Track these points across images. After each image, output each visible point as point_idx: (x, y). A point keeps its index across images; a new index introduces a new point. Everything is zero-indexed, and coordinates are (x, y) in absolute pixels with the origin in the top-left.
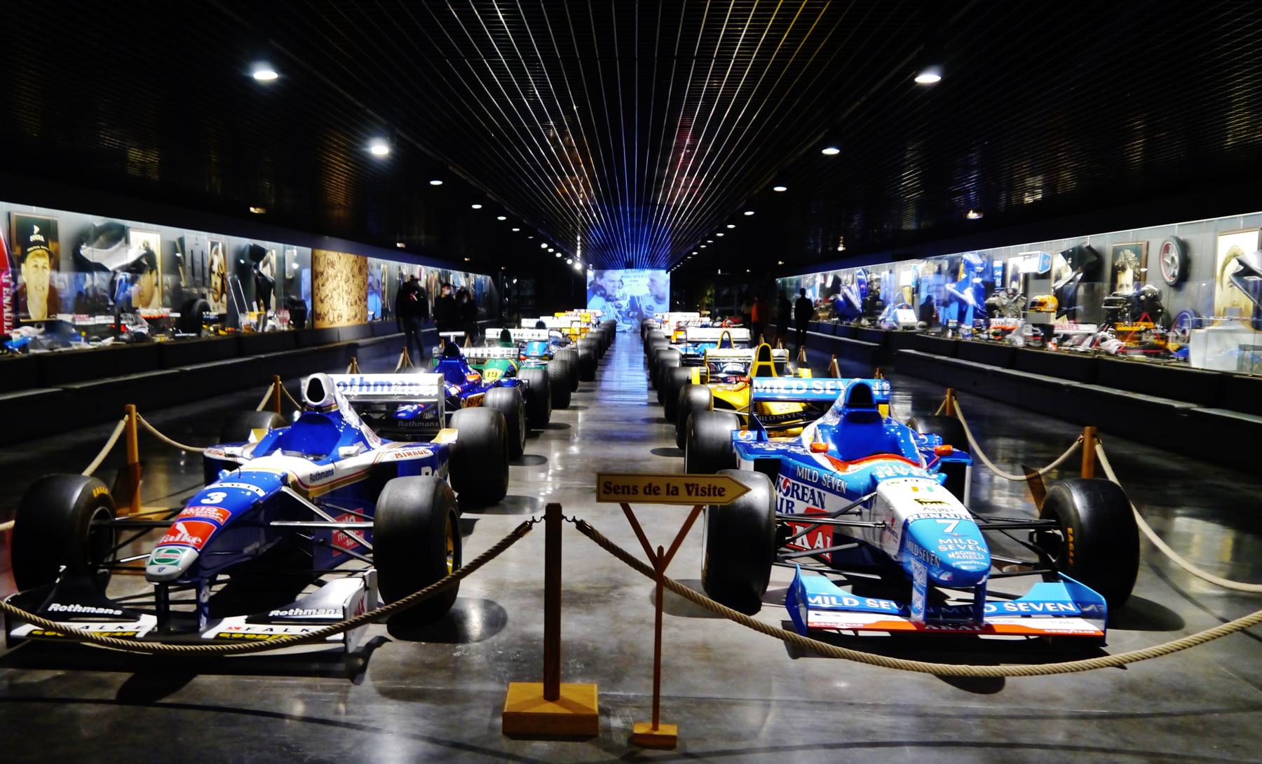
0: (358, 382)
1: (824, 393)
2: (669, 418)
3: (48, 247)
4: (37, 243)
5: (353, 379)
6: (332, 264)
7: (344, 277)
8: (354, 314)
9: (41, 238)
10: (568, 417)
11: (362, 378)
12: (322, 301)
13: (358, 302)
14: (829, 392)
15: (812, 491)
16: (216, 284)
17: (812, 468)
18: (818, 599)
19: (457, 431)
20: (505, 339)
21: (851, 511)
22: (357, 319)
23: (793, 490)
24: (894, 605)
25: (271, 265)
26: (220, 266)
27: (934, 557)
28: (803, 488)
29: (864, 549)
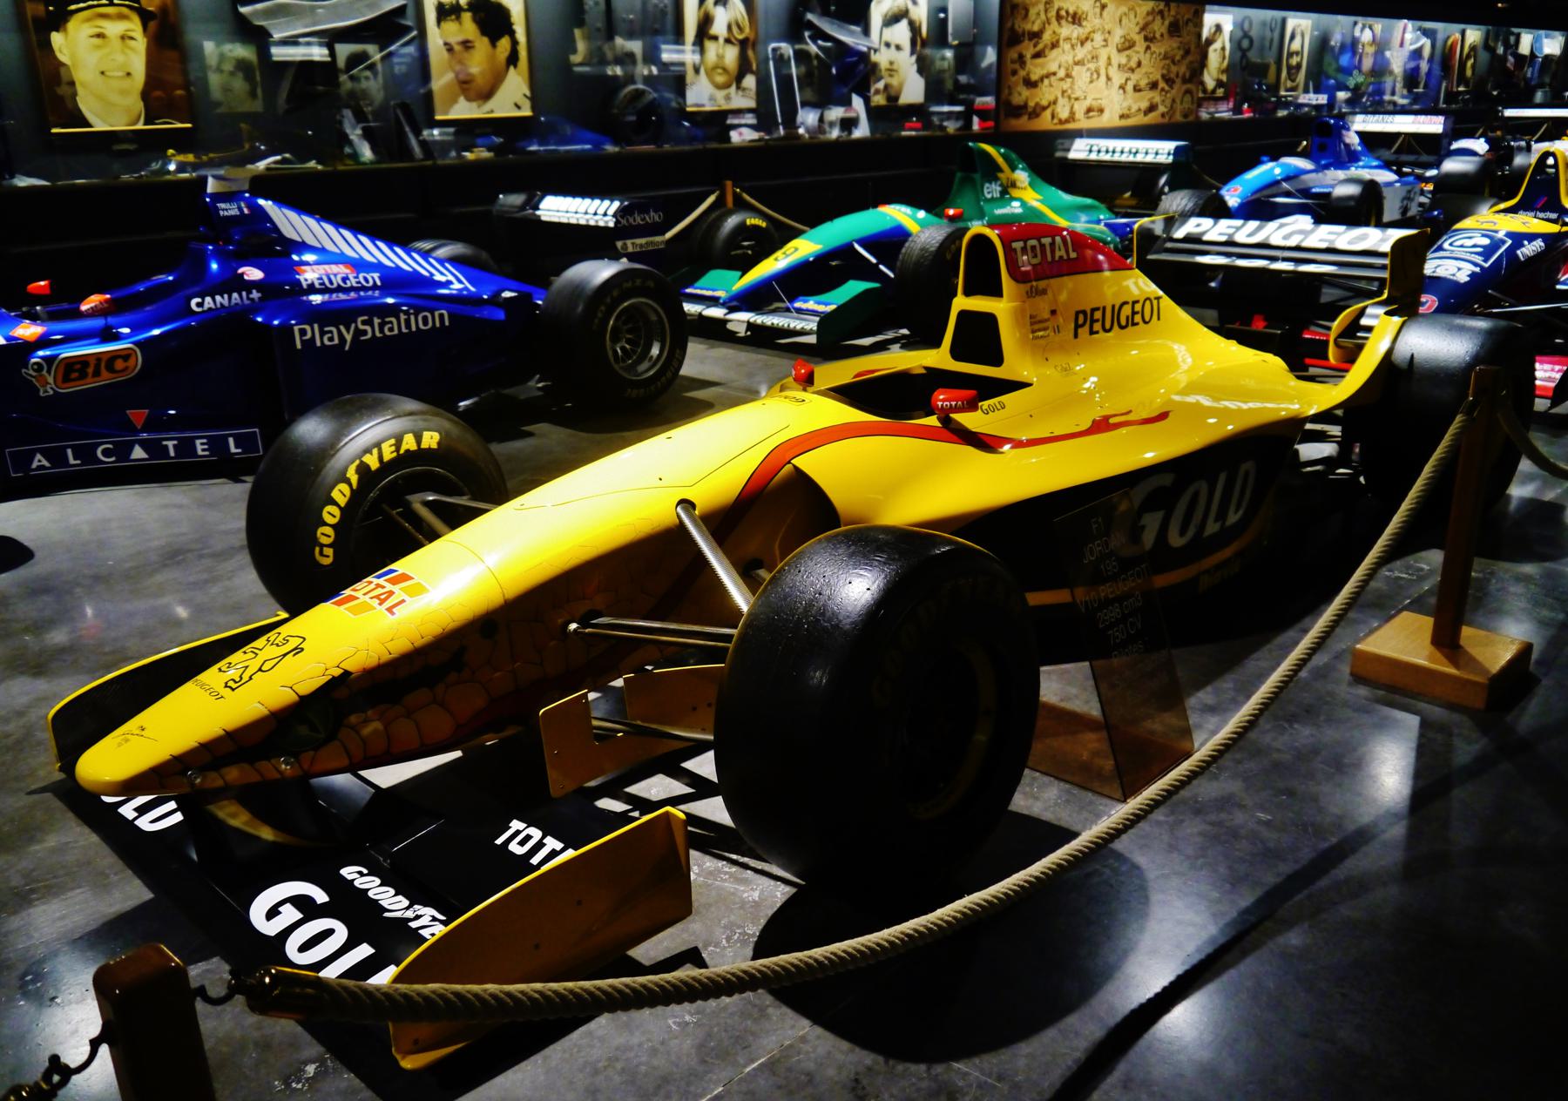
7: (1117, 37)
8: (1144, 105)
12: (1031, 84)
13: (1162, 84)
25: (912, 24)
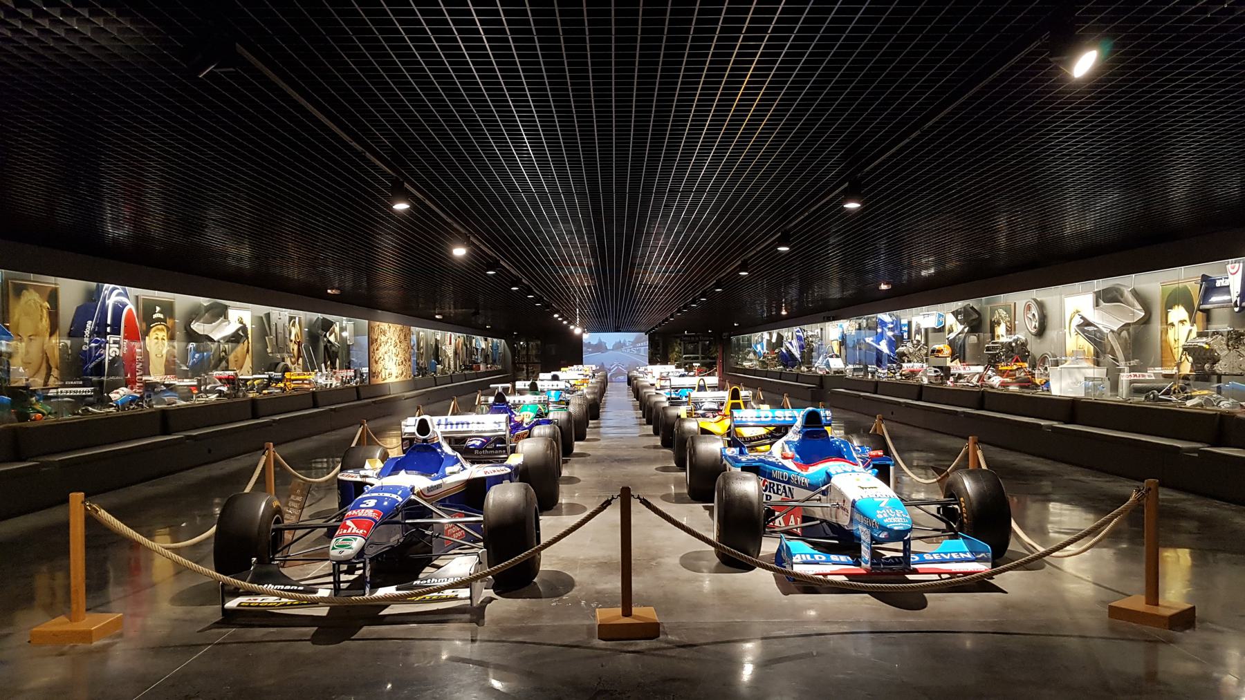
0: (443, 422)
1: (785, 420)
2: (666, 444)
3: (166, 323)
4: (158, 320)
5: (440, 420)
6: (384, 333)
7: (393, 342)
8: (401, 372)
9: (161, 316)
10: (587, 447)
11: (446, 419)
12: (376, 362)
14: (787, 419)
15: (784, 487)
16: (293, 350)
17: (784, 470)
18: (798, 556)
19: (522, 455)
20: (534, 389)
21: (813, 498)
22: (403, 376)
23: (770, 487)
24: (849, 558)
26: (296, 335)
27: (874, 523)
28: (778, 485)
29: (824, 524)
